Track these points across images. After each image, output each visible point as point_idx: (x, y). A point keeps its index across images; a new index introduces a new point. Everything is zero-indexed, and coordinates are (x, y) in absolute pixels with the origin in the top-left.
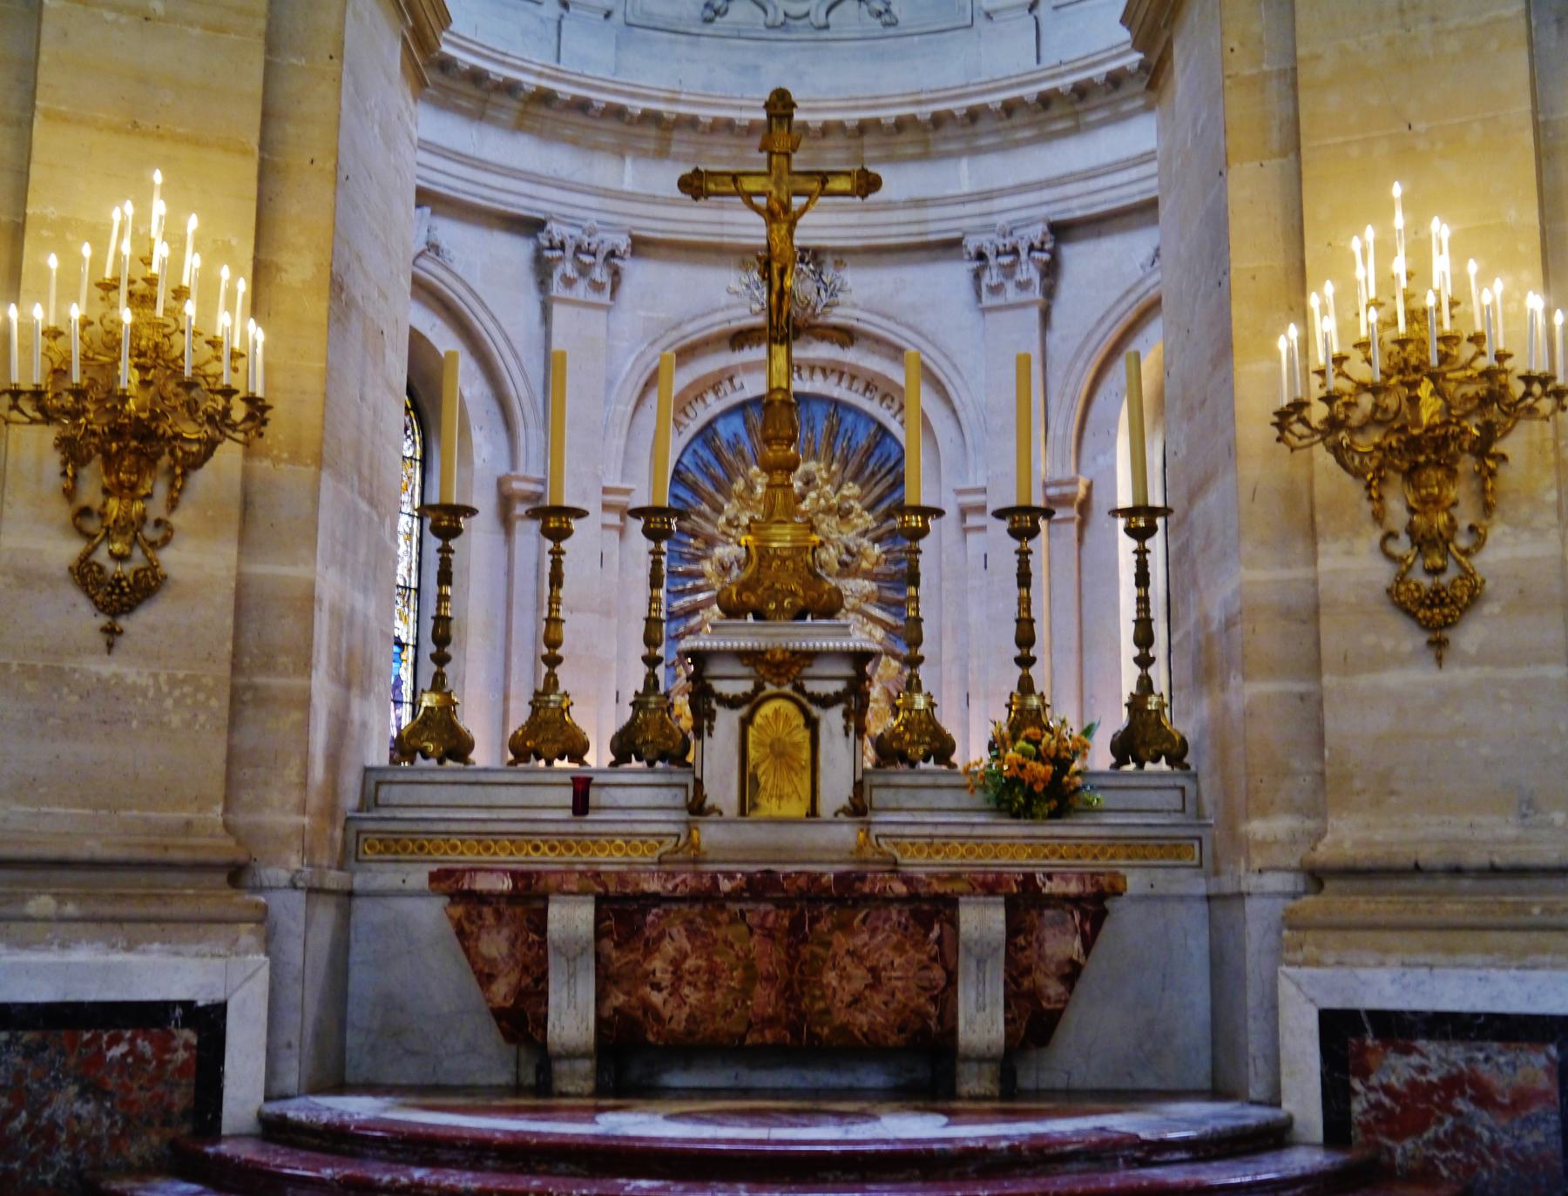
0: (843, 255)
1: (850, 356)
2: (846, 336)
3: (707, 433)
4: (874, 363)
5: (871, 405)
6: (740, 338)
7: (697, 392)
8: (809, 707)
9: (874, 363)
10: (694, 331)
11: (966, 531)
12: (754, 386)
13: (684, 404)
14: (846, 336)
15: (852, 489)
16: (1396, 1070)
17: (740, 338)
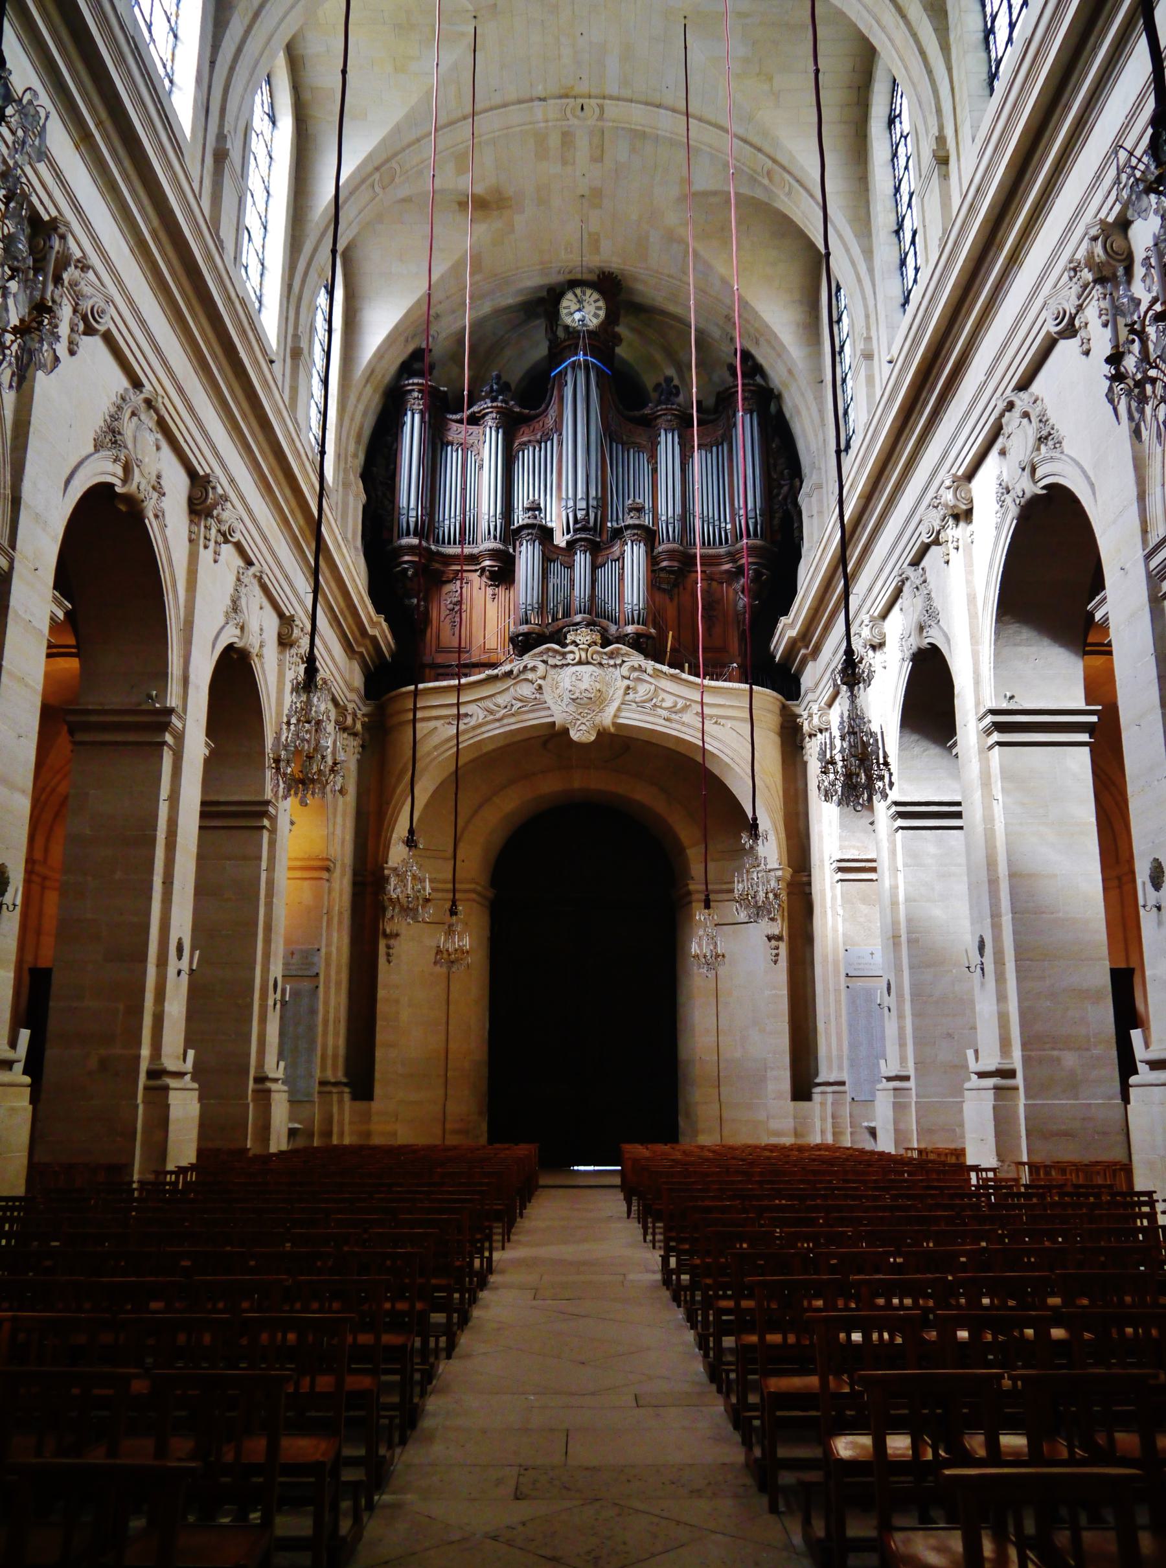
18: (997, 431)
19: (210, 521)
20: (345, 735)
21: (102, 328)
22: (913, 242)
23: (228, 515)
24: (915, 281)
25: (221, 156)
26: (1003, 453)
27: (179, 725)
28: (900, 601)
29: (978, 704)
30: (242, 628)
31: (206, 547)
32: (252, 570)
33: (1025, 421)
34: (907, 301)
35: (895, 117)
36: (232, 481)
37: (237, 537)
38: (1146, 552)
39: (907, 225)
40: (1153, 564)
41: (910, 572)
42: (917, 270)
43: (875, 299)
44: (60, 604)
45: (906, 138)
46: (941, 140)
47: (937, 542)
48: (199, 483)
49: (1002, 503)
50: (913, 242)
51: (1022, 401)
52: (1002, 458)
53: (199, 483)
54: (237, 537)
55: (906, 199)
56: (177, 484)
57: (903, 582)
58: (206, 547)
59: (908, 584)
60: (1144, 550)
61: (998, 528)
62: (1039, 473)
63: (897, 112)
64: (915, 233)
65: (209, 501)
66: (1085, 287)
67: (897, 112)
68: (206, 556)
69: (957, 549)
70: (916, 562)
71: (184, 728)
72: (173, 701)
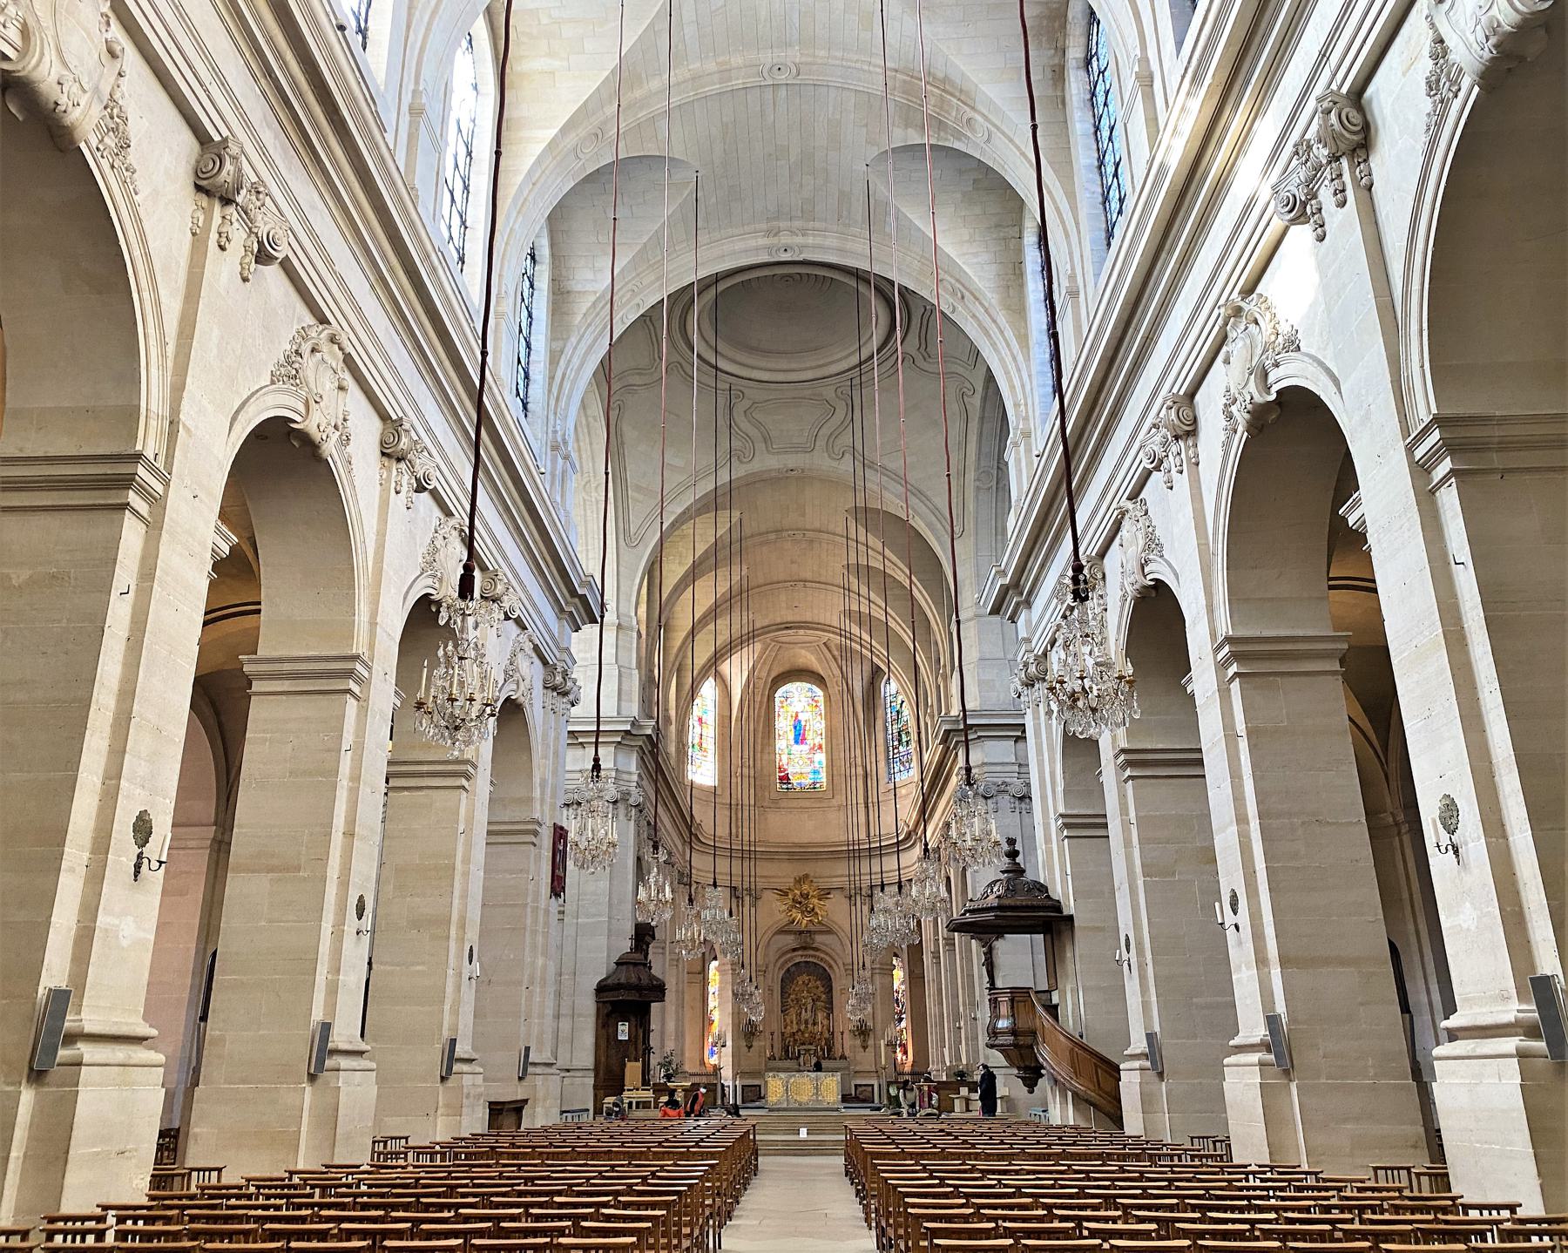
0: (815, 932)
1: (817, 953)
2: (816, 949)
3: (788, 970)
4: (822, 955)
5: (822, 964)
6: (794, 950)
7: (786, 962)
8: (810, 1055)
9: (822, 955)
10: (785, 949)
11: (842, 994)
12: (798, 960)
13: (783, 965)
14: (816, 949)
15: (818, 982)
16: (860, 1089)
17: (794, 950)
18: (1223, 339)
19: (402, 465)
20: (555, 694)
21: (281, 256)
22: (1116, 175)
23: (422, 465)
24: (1120, 212)
25: (416, 112)
26: (1227, 361)
27: (366, 675)
28: (1120, 533)
29: (1213, 635)
30: (441, 580)
31: (397, 493)
32: (452, 522)
33: (1252, 327)
34: (1110, 235)
35: (1092, 57)
36: (429, 430)
37: (434, 484)
38: (1408, 441)
39: (1109, 158)
40: (1419, 453)
41: (1130, 505)
42: (1121, 201)
43: (1079, 232)
44: (226, 539)
45: (1103, 72)
46: (1144, 60)
47: (1157, 469)
48: (391, 424)
49: (1230, 417)
50: (1116, 175)
51: (1249, 306)
52: (1227, 366)
53: (391, 424)
54: (434, 484)
55: (1106, 134)
56: (366, 430)
57: (1123, 514)
58: (397, 493)
59: (1127, 517)
60: (1404, 439)
61: (1227, 446)
62: (1271, 378)
63: (1093, 52)
64: (1117, 165)
65: (401, 445)
66: (1318, 168)
67: (1093, 52)
68: (397, 502)
69: (1181, 472)
70: (1133, 497)
71: (370, 673)
72: (359, 647)
